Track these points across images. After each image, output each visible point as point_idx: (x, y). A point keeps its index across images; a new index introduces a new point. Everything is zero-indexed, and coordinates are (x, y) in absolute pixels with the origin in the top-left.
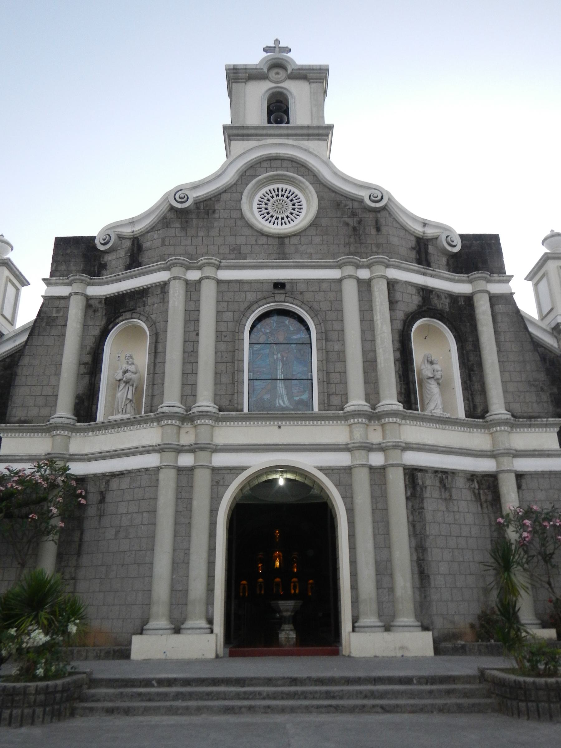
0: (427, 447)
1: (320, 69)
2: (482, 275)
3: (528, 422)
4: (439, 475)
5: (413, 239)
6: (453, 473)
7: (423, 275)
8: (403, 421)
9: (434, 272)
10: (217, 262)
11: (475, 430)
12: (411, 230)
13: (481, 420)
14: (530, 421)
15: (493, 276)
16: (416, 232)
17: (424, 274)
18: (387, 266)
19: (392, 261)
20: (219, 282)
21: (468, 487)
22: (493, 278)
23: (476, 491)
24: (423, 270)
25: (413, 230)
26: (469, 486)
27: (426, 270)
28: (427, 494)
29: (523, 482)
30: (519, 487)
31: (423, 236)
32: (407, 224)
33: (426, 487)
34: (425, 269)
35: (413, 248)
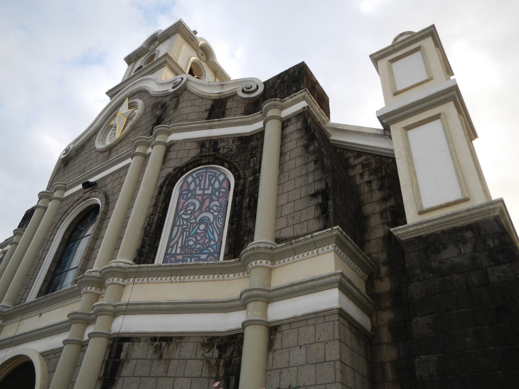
0: (142, 307)
1: (175, 24)
2: (269, 104)
3: (290, 247)
4: (157, 343)
5: (211, 101)
6: (181, 338)
7: (210, 129)
8: (126, 281)
9: (221, 122)
10: (62, 185)
11: (231, 276)
12: (206, 96)
13: (233, 260)
14: (291, 244)
15: (285, 100)
16: (211, 95)
17: (210, 128)
18: (169, 134)
19: (172, 127)
20: (62, 200)
21: (199, 357)
22: (285, 103)
23: (213, 362)
24: (208, 124)
25: (207, 95)
26: (203, 355)
27: (210, 123)
28: (127, 370)
29: (279, 336)
30: (270, 345)
31: (220, 97)
32: (202, 92)
33: (128, 362)
34: (209, 122)
35: (206, 110)
